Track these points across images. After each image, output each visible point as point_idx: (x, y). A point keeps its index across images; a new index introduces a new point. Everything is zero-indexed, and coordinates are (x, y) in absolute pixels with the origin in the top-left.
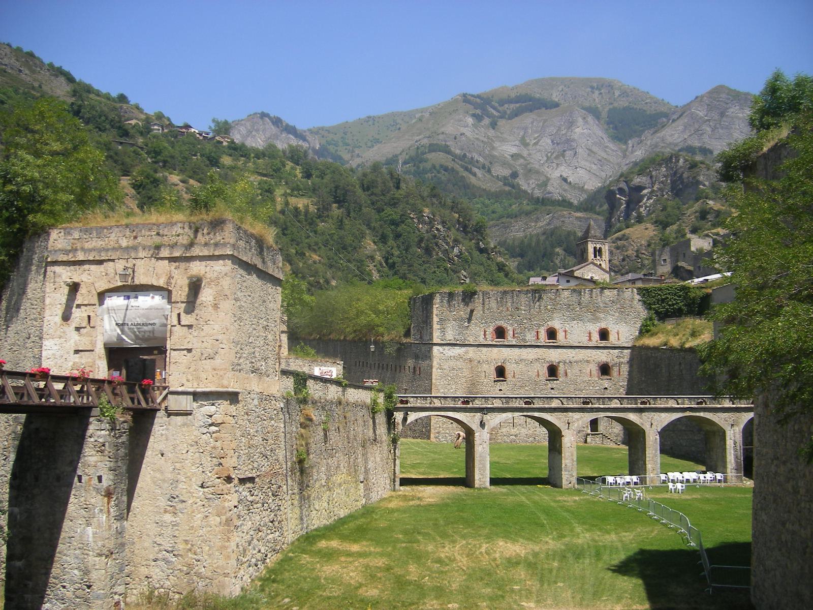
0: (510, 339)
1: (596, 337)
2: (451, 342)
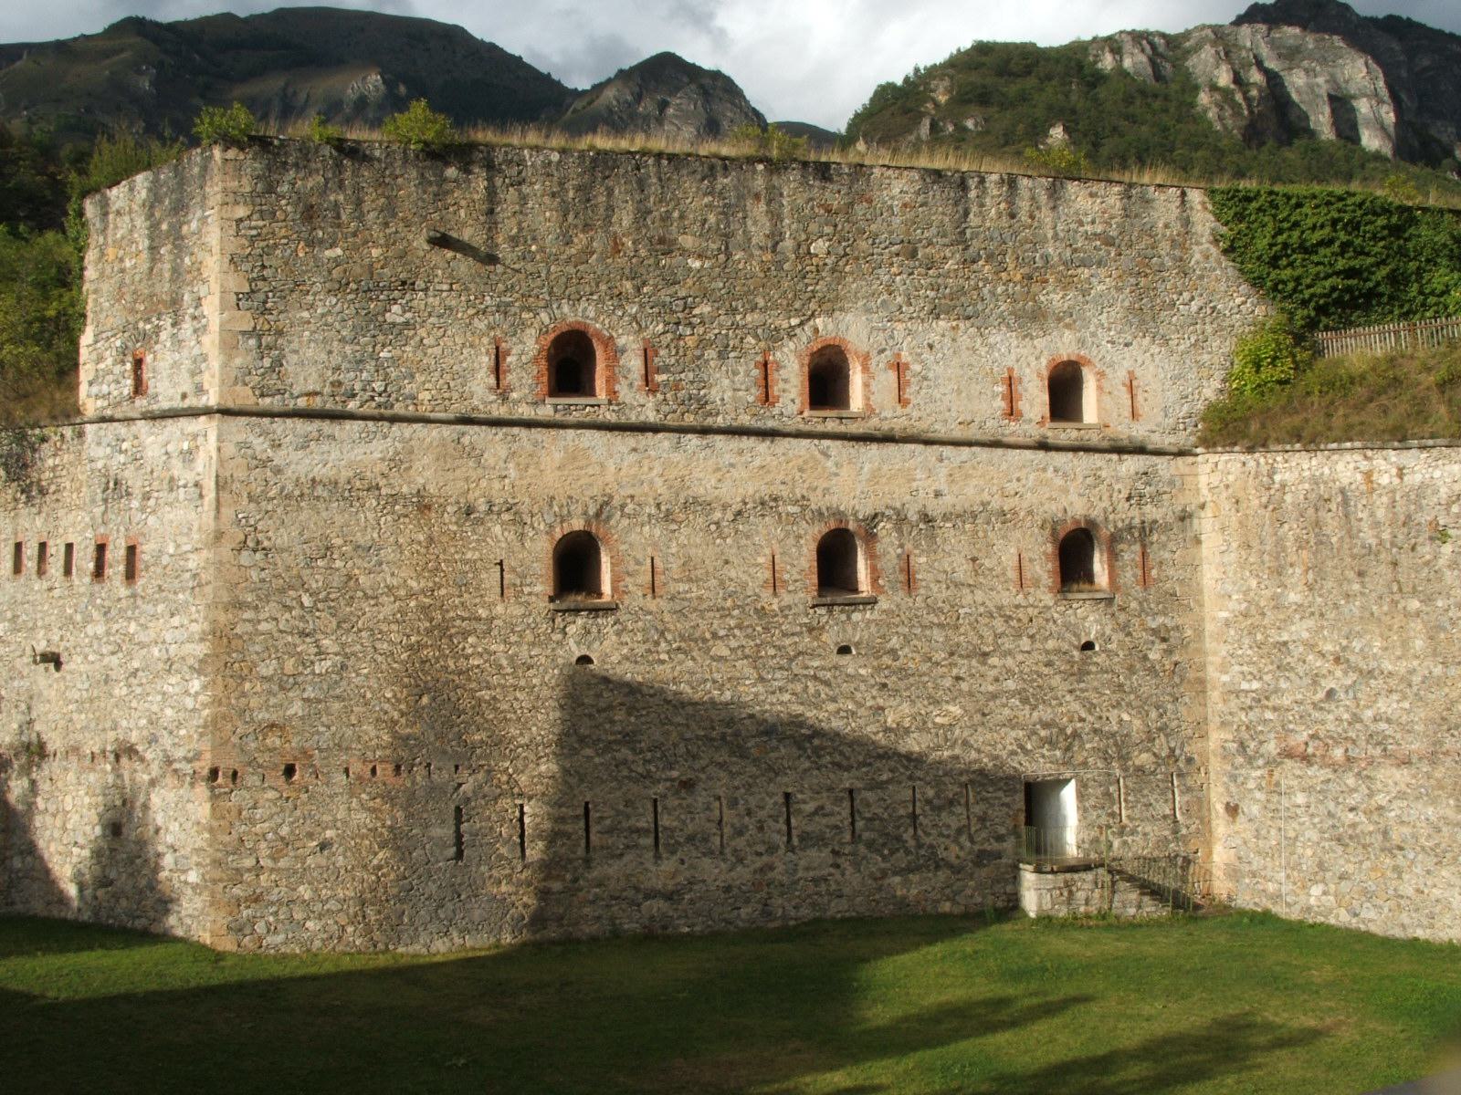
0: (625, 393)
1: (1036, 400)
2: (317, 403)
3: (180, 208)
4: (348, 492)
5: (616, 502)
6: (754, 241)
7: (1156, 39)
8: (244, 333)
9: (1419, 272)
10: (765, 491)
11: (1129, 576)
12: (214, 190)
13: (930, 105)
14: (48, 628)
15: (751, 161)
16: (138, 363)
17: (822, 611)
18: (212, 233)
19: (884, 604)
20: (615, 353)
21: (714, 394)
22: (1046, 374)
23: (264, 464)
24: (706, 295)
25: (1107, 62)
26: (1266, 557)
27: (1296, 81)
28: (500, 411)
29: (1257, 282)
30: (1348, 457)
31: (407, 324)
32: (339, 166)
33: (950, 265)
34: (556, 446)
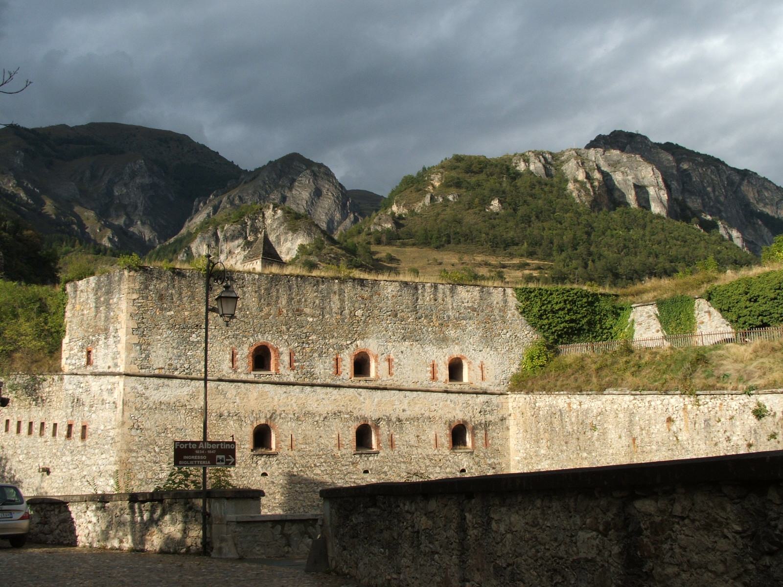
0: (282, 370)
1: (443, 373)
2: (163, 372)
3: (109, 292)
4: (174, 407)
5: (278, 413)
6: (334, 310)
7: (547, 155)
8: (135, 344)
9: (600, 320)
10: (336, 409)
11: (480, 443)
12: (125, 287)
13: (430, 188)
14: (44, 458)
15: (333, 278)
16: (89, 352)
17: (357, 456)
18: (123, 304)
19: (382, 454)
20: (278, 355)
21: (317, 371)
22: (447, 363)
23: (141, 395)
24: (314, 332)
25: (522, 167)
26: (533, 436)
27: (618, 177)
28: (233, 377)
29: (534, 325)
30: (562, 397)
31: (198, 341)
32: (173, 279)
33: (410, 320)
34: (254, 391)
